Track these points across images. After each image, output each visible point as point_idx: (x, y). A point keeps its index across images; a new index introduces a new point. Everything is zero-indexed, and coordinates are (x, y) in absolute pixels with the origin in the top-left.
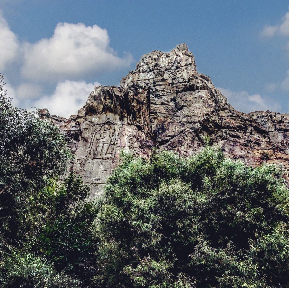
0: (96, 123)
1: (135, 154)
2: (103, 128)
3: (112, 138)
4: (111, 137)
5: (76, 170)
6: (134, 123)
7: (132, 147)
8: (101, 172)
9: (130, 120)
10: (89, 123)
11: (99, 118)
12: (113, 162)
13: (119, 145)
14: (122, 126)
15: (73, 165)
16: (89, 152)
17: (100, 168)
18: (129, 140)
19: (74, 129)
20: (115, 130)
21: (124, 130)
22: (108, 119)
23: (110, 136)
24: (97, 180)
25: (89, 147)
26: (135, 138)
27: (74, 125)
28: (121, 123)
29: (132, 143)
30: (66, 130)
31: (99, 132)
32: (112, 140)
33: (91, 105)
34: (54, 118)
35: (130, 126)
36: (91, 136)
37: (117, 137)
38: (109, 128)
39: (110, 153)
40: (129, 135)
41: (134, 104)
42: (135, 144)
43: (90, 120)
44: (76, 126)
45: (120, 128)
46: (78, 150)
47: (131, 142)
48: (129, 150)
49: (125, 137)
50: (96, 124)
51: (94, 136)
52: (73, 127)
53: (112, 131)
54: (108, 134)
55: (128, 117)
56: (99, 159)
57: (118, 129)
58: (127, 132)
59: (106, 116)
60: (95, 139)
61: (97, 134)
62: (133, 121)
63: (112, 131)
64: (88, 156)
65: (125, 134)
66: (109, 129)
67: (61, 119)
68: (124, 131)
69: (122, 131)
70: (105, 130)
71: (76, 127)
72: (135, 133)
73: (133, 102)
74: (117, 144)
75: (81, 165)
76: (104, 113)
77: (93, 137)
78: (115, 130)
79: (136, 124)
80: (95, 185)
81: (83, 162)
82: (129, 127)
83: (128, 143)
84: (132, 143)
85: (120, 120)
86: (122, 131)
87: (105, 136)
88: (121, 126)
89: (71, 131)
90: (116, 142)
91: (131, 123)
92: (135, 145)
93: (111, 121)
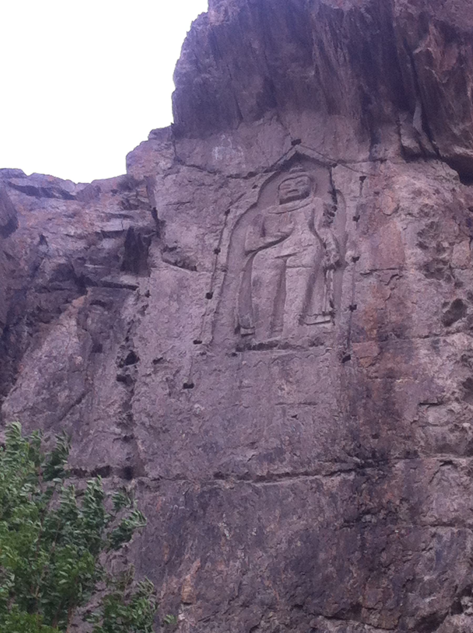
0: (234, 172)
1: (464, 298)
2: (272, 187)
3: (328, 235)
4: (321, 231)
5: (148, 415)
6: (434, 146)
7: (439, 270)
8: (284, 411)
9: (416, 136)
10: (197, 175)
11: (249, 146)
12: (348, 358)
13: (366, 264)
14: (374, 168)
15: (132, 392)
16: (209, 318)
17: (280, 393)
18: (420, 234)
19: (115, 225)
20: (334, 193)
21: (388, 186)
22: (296, 142)
23: (311, 226)
24: (269, 458)
25: (209, 296)
26: (454, 218)
27: (115, 209)
28: (364, 155)
29: (440, 249)
30: (79, 232)
31: (253, 214)
32: (325, 246)
33: (197, 80)
34: (14, 181)
35: (416, 165)
36: (212, 241)
37: (350, 226)
38: (302, 188)
39: (324, 314)
40: (415, 210)
41: (429, 44)
42: (456, 248)
43: (198, 161)
44: (123, 212)
45: (362, 179)
46: (152, 313)
47: (434, 244)
48: (430, 284)
49: (398, 223)
50: (231, 176)
51: (226, 234)
52: (110, 217)
53: (318, 202)
54: (302, 217)
55: (403, 116)
56: (270, 346)
57: (355, 187)
58: (404, 193)
59: (280, 128)
60: (237, 251)
61: (244, 222)
62: (430, 139)
63: (318, 202)
64: (205, 339)
65: (393, 206)
66: (306, 195)
67: (45, 186)
68: (387, 192)
69: (377, 193)
70: (281, 203)
71: (125, 217)
72: (448, 196)
73: (421, 37)
74: (355, 259)
75: (172, 387)
76: (268, 115)
77: (226, 243)
78: (334, 193)
79: (446, 151)
80: (258, 485)
81: (182, 372)
82: (413, 173)
83: (419, 251)
84: (440, 249)
85: (361, 142)
86: (377, 193)
87: (286, 229)
88: (365, 168)
89: (105, 235)
90: (350, 253)
91: (416, 151)
92: (455, 256)
93: (308, 152)
